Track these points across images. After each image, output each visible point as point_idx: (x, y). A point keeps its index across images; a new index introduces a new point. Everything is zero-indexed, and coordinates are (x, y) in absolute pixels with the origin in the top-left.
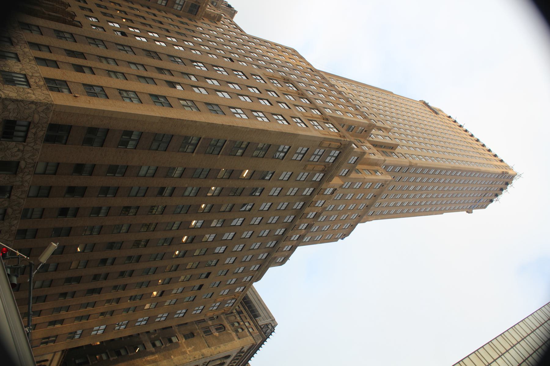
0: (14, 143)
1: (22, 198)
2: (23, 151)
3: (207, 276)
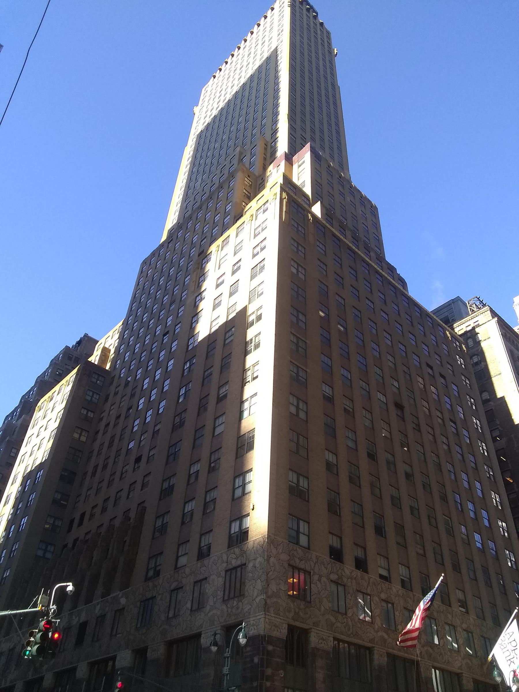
1: (369, 580)
2: (320, 576)
3: (431, 368)
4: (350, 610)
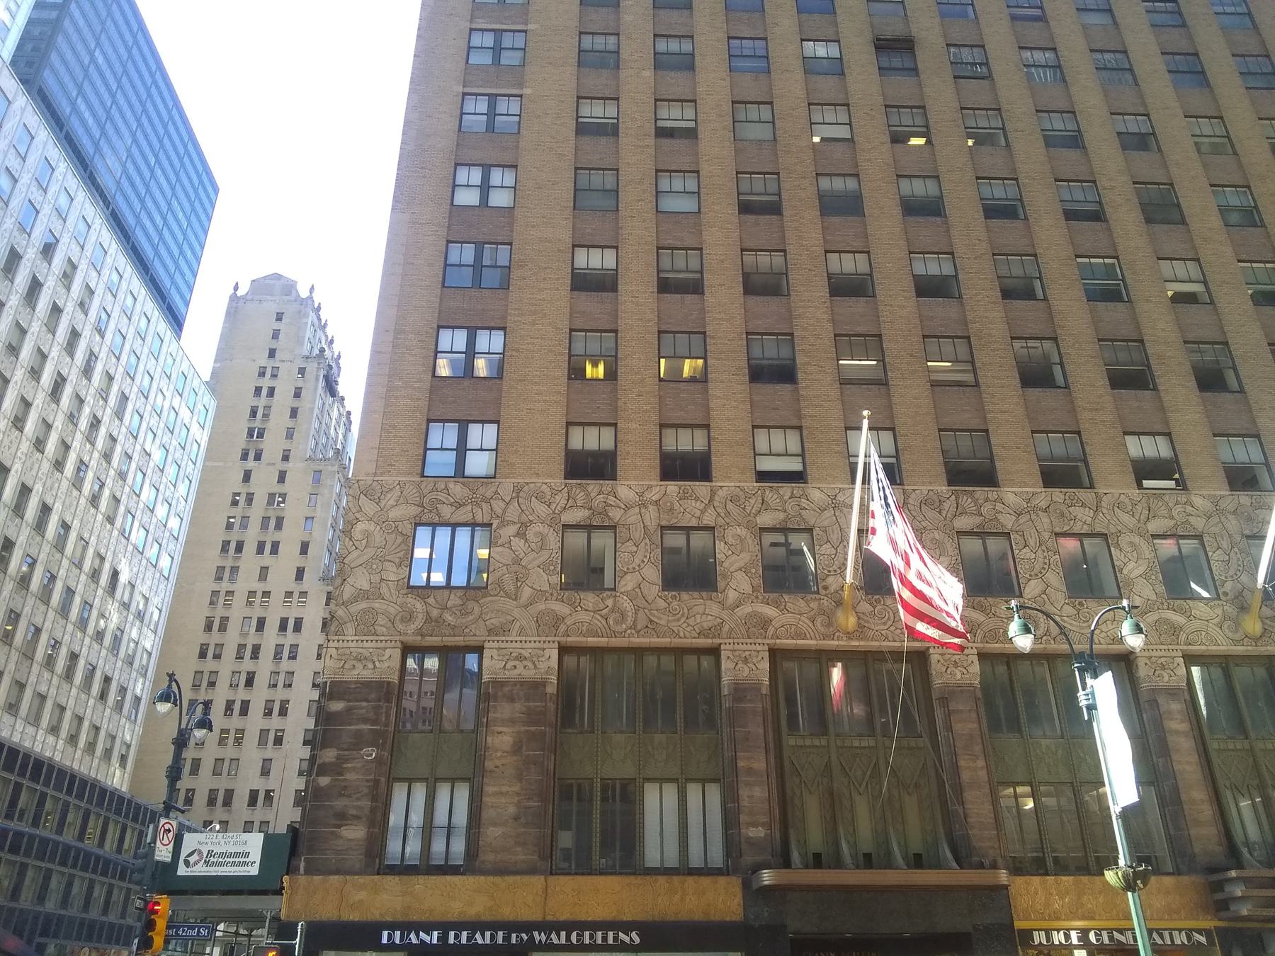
4: (628, 577)
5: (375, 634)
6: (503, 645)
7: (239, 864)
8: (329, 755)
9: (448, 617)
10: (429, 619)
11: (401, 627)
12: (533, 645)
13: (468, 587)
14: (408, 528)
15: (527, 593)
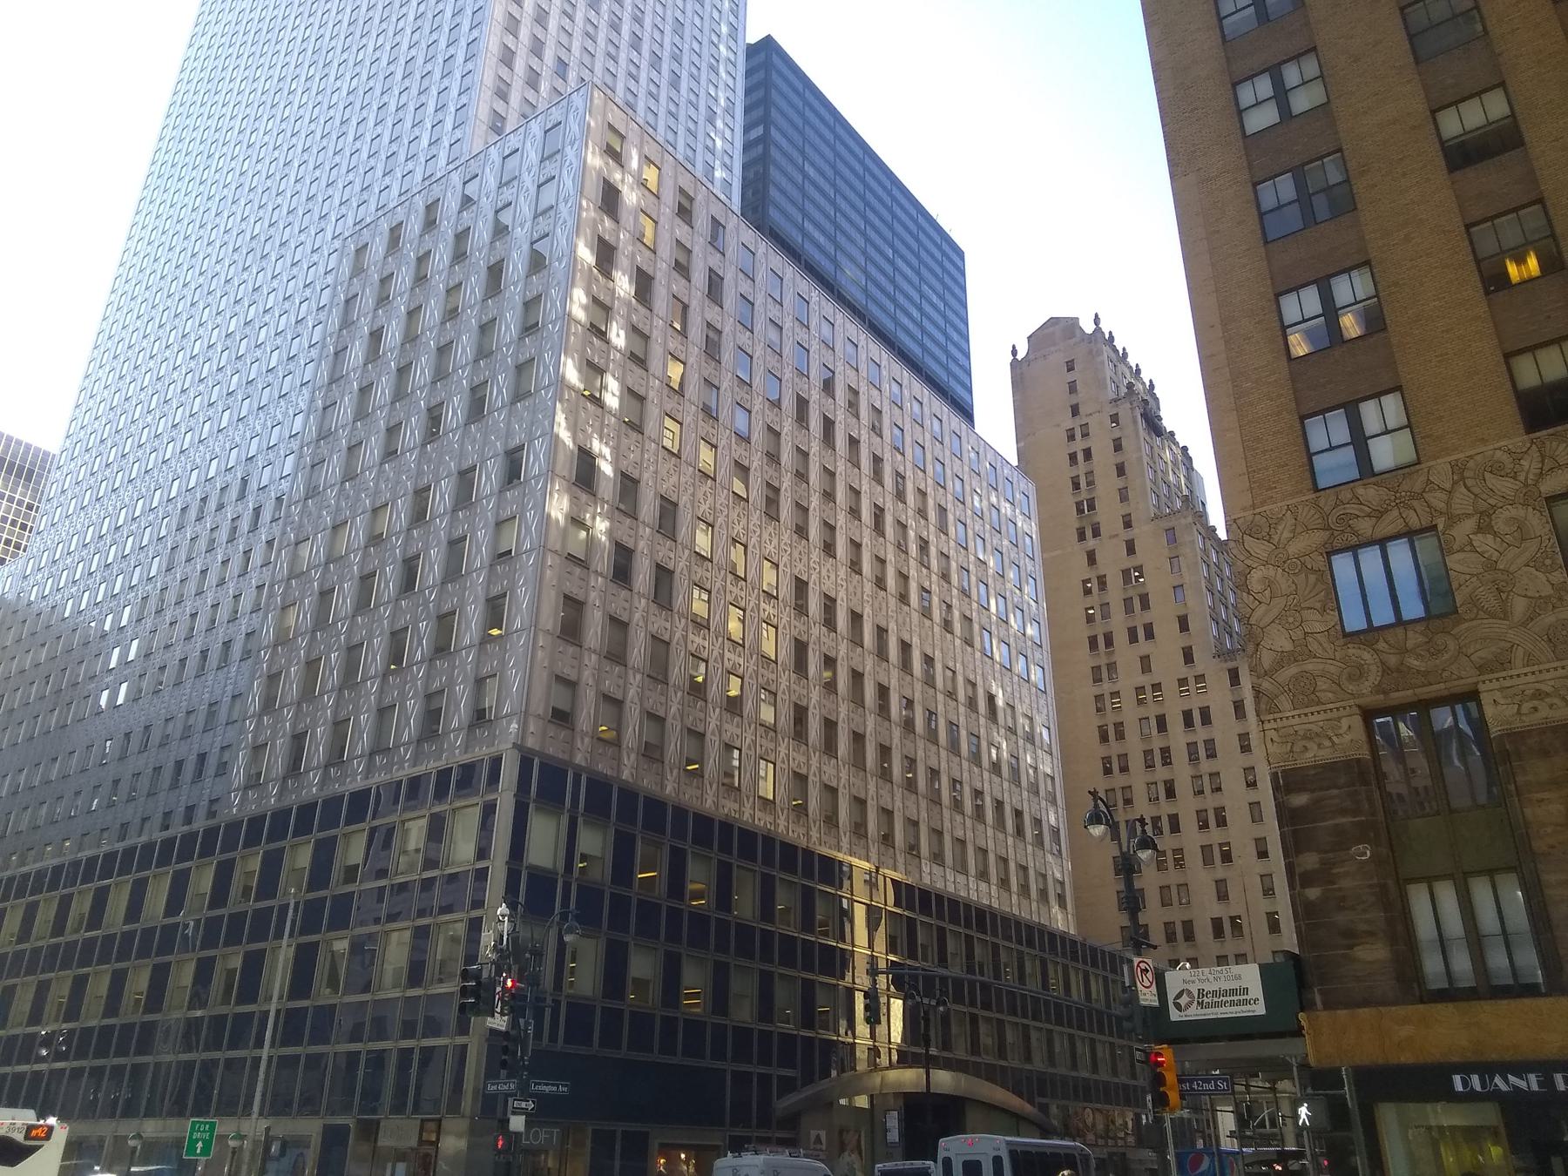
0: (1453, 561)
5: (1319, 703)
6: (1508, 683)
7: (1239, 1003)
8: (1310, 861)
9: (1414, 662)
10: (1386, 669)
11: (1351, 688)
12: (1552, 674)
13: (1429, 617)
14: (1320, 562)
15: (1519, 606)
